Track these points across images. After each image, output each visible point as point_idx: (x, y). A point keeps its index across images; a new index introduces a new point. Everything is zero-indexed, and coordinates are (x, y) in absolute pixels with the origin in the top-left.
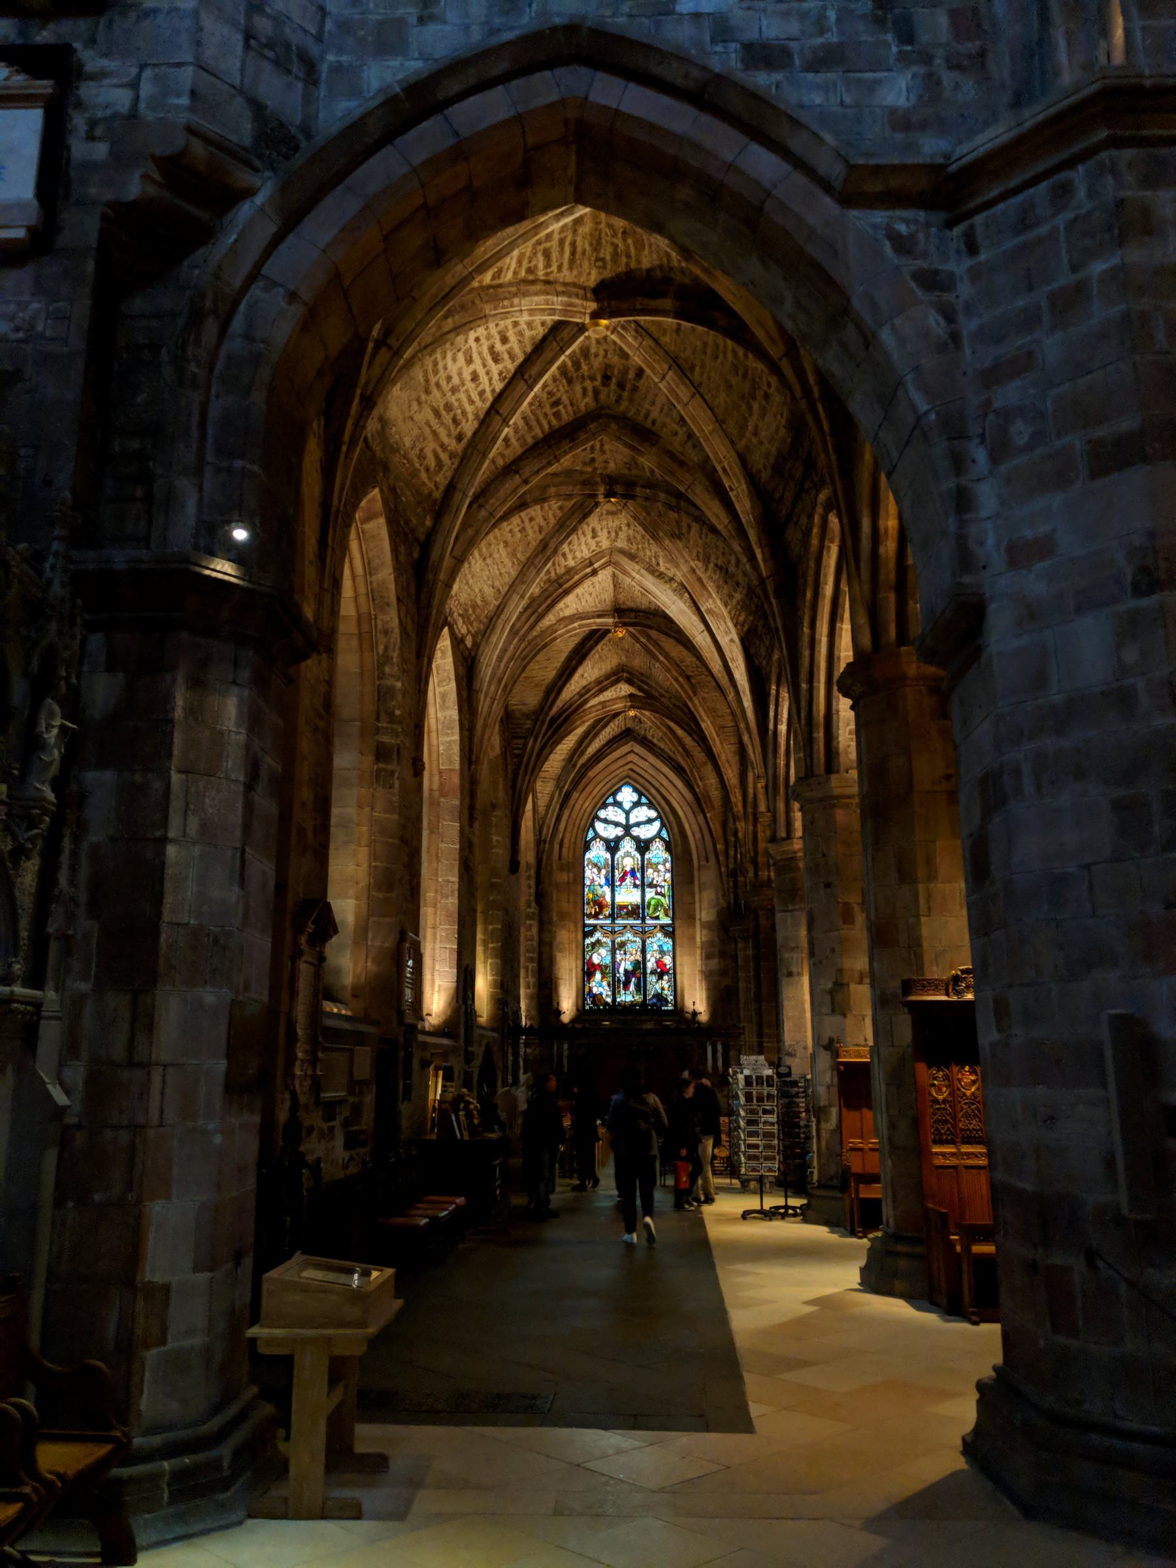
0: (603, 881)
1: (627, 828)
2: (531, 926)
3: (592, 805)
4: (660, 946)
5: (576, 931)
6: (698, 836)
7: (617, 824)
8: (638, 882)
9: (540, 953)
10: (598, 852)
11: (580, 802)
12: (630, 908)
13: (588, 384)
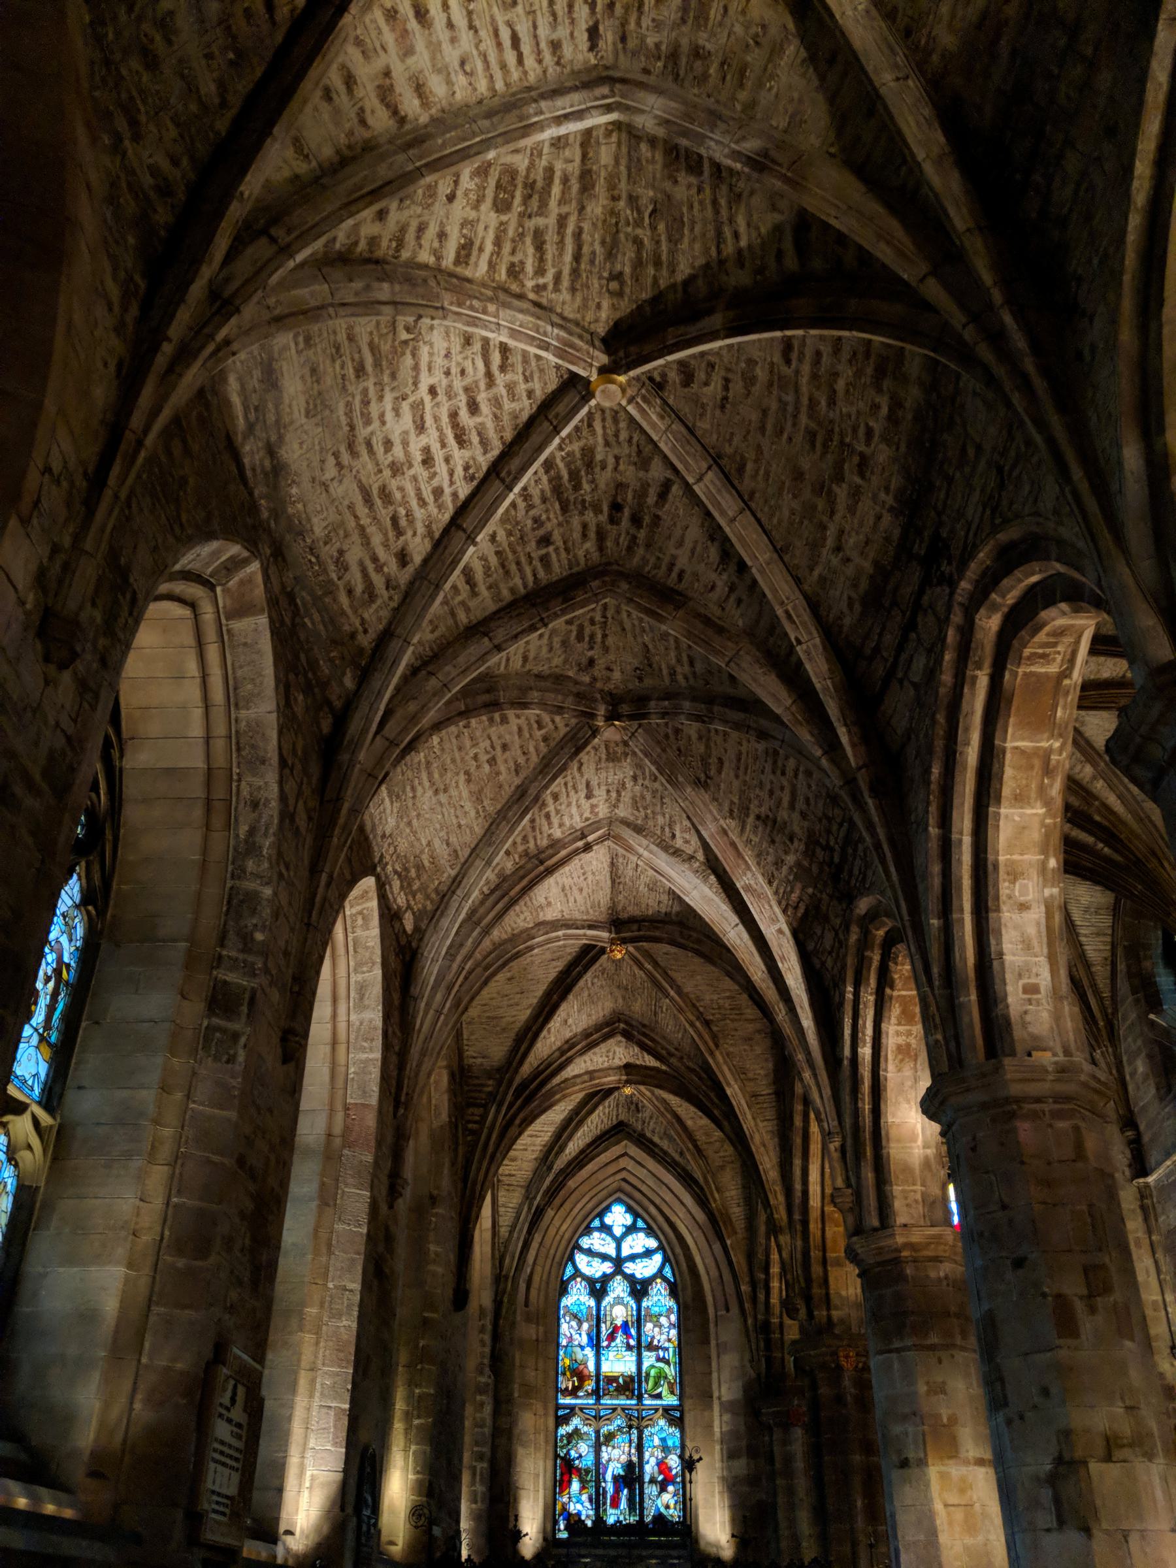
0: (584, 1340)
1: (618, 1262)
2: (482, 1404)
3: (571, 1230)
4: (663, 1440)
5: (546, 1415)
6: (714, 1273)
7: (604, 1257)
8: (632, 1342)
9: (494, 1448)
10: (577, 1298)
11: (557, 1222)
13: (589, 516)
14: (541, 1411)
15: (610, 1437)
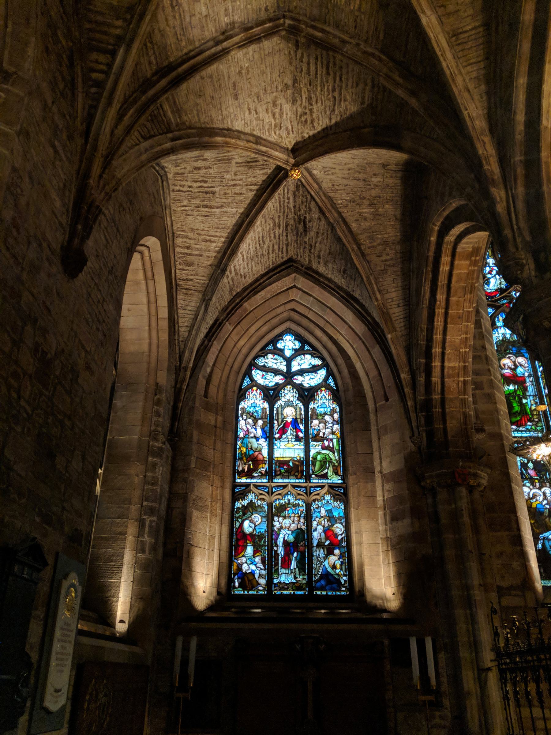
0: (259, 432)
1: (289, 376)
3: (248, 346)
4: (329, 511)
5: (223, 487)
6: (373, 373)
7: (277, 372)
8: (301, 435)
9: (169, 508)
11: (235, 337)
12: (291, 464)
14: (218, 483)
15: (282, 509)
